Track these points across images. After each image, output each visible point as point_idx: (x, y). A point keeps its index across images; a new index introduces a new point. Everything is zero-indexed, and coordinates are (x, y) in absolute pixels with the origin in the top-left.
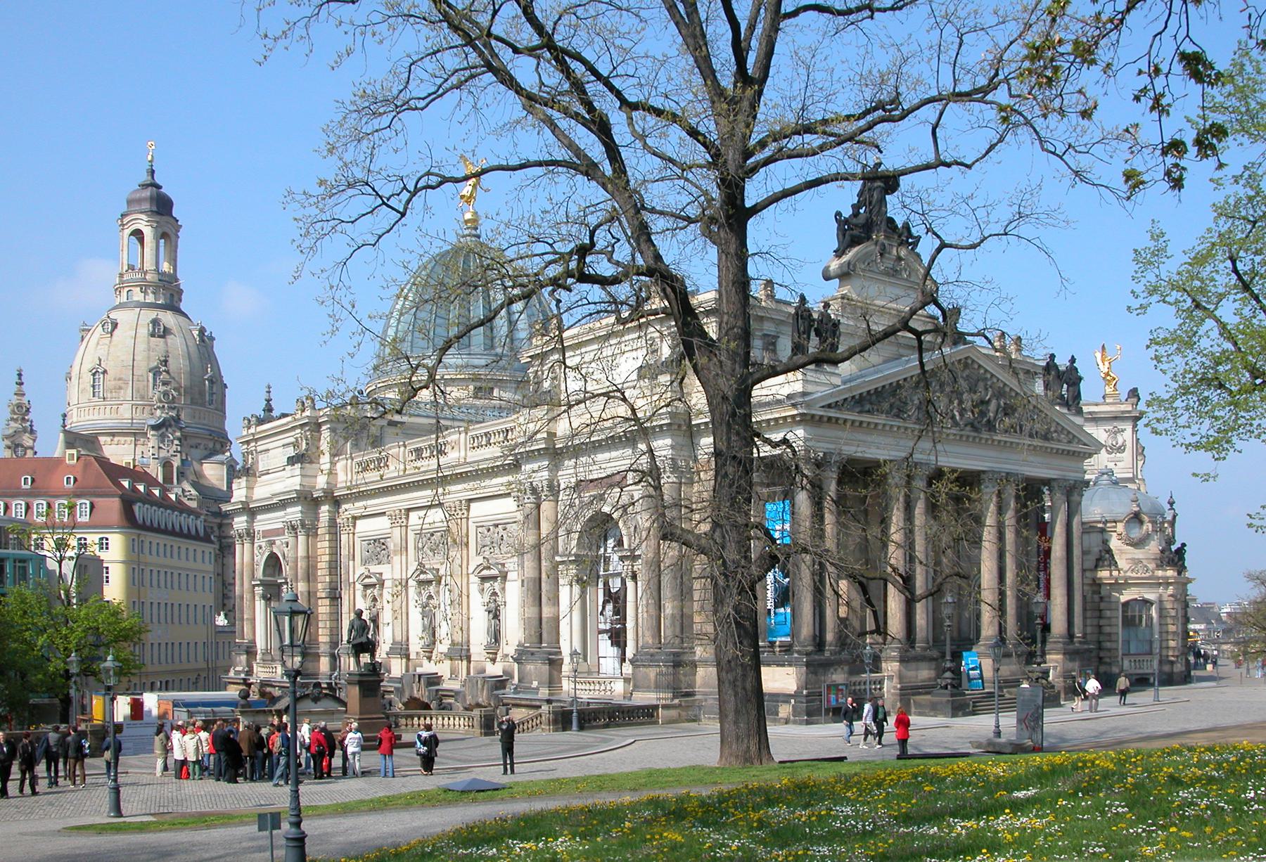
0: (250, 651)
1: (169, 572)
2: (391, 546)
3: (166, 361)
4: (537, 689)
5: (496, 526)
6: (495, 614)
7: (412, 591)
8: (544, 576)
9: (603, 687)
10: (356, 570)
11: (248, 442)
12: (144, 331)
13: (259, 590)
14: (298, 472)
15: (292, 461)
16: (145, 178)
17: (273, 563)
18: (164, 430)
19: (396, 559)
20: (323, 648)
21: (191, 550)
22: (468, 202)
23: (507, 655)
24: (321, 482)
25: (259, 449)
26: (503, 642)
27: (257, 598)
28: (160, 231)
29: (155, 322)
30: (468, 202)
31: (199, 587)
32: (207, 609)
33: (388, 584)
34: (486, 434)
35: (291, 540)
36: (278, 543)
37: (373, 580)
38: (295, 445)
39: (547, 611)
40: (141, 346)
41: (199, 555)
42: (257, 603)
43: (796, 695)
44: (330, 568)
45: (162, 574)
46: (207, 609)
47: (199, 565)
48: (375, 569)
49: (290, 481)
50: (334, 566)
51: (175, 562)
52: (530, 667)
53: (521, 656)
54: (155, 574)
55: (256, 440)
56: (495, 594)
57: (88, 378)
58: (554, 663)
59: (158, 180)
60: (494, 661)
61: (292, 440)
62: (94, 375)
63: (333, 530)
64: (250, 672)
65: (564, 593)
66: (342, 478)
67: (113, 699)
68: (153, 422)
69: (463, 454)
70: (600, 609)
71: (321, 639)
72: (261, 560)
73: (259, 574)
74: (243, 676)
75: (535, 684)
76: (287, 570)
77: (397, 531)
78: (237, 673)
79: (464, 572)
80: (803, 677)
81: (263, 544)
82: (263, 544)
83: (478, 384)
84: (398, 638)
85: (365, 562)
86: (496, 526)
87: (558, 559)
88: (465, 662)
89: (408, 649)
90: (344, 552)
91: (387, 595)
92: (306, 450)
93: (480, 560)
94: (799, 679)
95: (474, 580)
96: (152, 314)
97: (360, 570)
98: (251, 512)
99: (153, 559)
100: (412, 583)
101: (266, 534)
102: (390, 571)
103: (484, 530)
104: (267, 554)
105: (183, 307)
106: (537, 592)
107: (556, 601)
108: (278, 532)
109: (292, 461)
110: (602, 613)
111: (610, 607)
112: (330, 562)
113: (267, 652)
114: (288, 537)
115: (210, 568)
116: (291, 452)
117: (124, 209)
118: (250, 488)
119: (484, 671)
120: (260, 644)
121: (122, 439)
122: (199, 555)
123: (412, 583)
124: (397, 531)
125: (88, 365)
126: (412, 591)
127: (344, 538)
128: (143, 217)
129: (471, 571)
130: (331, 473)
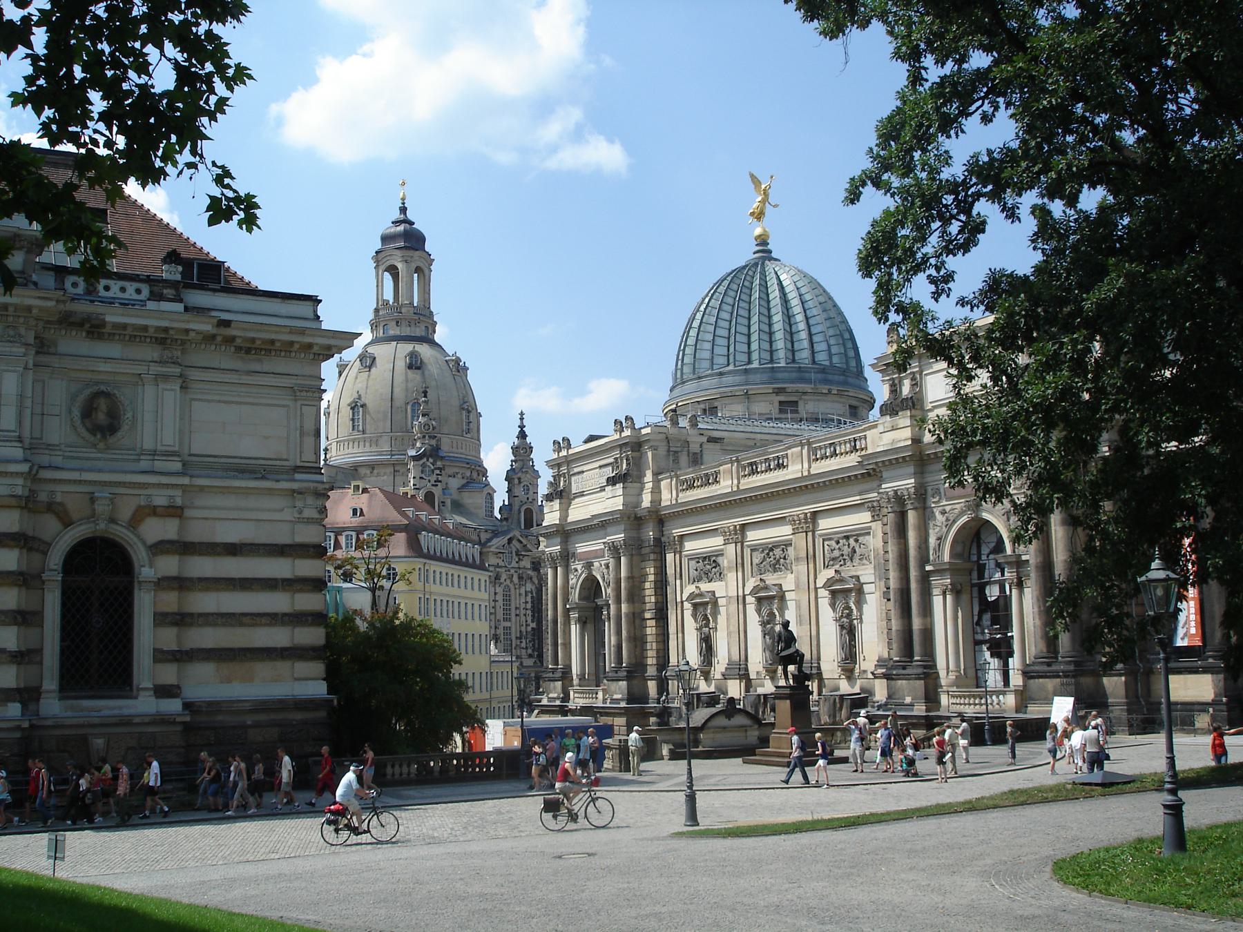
0: (566, 675)
3: (425, 394)
4: (912, 705)
5: (847, 538)
6: (849, 631)
9: (983, 701)
10: (683, 590)
11: (559, 465)
12: (401, 364)
13: (574, 615)
14: (620, 492)
15: (612, 481)
16: (397, 215)
17: (592, 588)
19: (731, 576)
20: (651, 671)
22: (759, 218)
23: (865, 671)
26: (860, 657)
27: (573, 622)
28: (414, 266)
29: (413, 355)
30: (759, 218)
32: (483, 638)
36: (596, 564)
40: (399, 378)
42: (573, 627)
43: (1214, 703)
46: (483, 638)
47: (476, 594)
48: (705, 587)
49: (613, 501)
50: (662, 585)
57: (346, 412)
58: (929, 674)
59: (410, 216)
61: (611, 460)
62: (353, 408)
63: (658, 550)
64: (566, 698)
65: (937, 601)
66: (667, 498)
67: (889, 697)
68: (412, 453)
70: (976, 618)
71: (650, 661)
73: (575, 596)
74: (558, 703)
75: (908, 700)
76: (608, 592)
77: (731, 549)
78: (550, 699)
79: (812, 586)
80: (1221, 684)
81: (579, 567)
82: (579, 567)
83: (782, 398)
84: (736, 657)
86: (847, 538)
87: (928, 568)
89: (747, 669)
93: (830, 573)
94: (1215, 686)
95: (823, 593)
96: (409, 347)
97: (690, 589)
98: (565, 533)
99: (435, 588)
100: (750, 600)
102: (724, 588)
103: (833, 543)
104: (584, 576)
105: (437, 338)
106: (907, 603)
107: (927, 610)
108: (598, 554)
109: (612, 481)
110: (978, 623)
111: (987, 618)
115: (486, 596)
116: (609, 472)
117: (379, 246)
119: (837, 689)
120: (575, 670)
121: (382, 471)
123: (750, 599)
125: (347, 399)
127: (670, 557)
128: (398, 252)
129: (820, 583)
130: (656, 490)
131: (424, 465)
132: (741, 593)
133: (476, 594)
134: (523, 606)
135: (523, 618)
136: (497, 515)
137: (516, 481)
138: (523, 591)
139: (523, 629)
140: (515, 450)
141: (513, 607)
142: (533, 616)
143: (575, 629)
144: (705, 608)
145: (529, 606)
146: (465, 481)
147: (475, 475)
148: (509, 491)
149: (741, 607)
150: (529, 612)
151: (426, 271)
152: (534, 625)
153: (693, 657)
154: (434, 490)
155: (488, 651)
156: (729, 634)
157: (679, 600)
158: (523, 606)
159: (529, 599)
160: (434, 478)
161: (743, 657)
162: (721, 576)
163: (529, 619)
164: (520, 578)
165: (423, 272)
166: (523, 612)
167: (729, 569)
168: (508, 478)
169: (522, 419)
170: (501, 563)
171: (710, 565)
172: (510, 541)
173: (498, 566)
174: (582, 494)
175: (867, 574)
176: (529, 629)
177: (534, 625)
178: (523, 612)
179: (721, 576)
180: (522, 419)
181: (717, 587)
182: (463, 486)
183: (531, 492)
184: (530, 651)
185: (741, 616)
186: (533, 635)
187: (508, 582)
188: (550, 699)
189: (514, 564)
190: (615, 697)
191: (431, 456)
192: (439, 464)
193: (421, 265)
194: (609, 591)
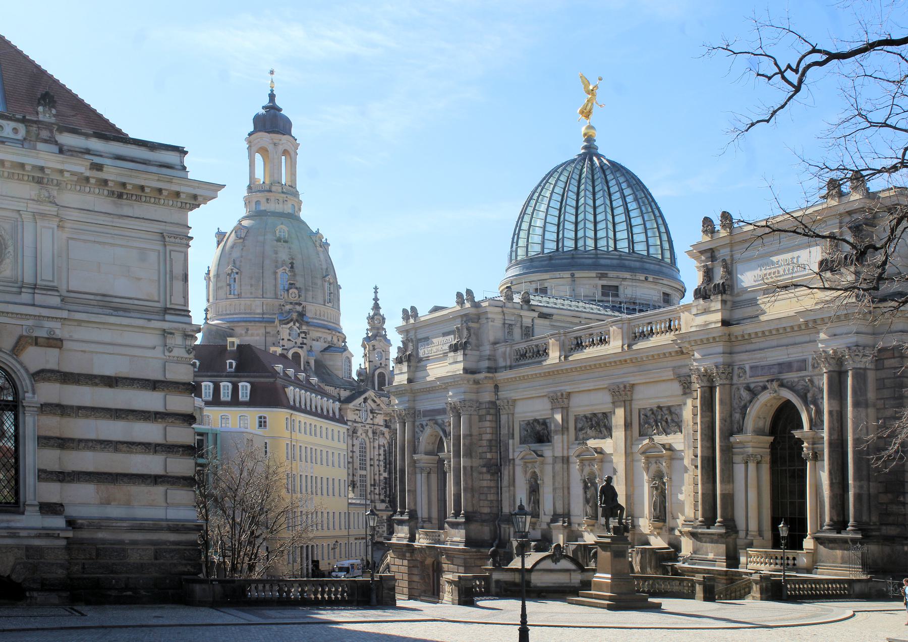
1: (309, 447)
18: (292, 324)
131: (290, 329)
133: (335, 444)
134: (376, 457)
135: (377, 468)
136: (355, 376)
138: (376, 445)
139: (377, 477)
140: (371, 319)
142: (385, 467)
145: (382, 458)
146: (326, 345)
150: (382, 463)
152: (386, 475)
155: (346, 496)
158: (376, 457)
159: (382, 452)
163: (382, 469)
164: (374, 433)
169: (376, 292)
170: (358, 420)
172: (365, 400)
173: (355, 422)
176: (382, 478)
177: (386, 475)
178: (376, 463)
180: (376, 292)
182: (326, 349)
183: (384, 359)
184: (382, 497)
186: (386, 483)
187: (364, 435)
189: (369, 421)
191: (297, 321)
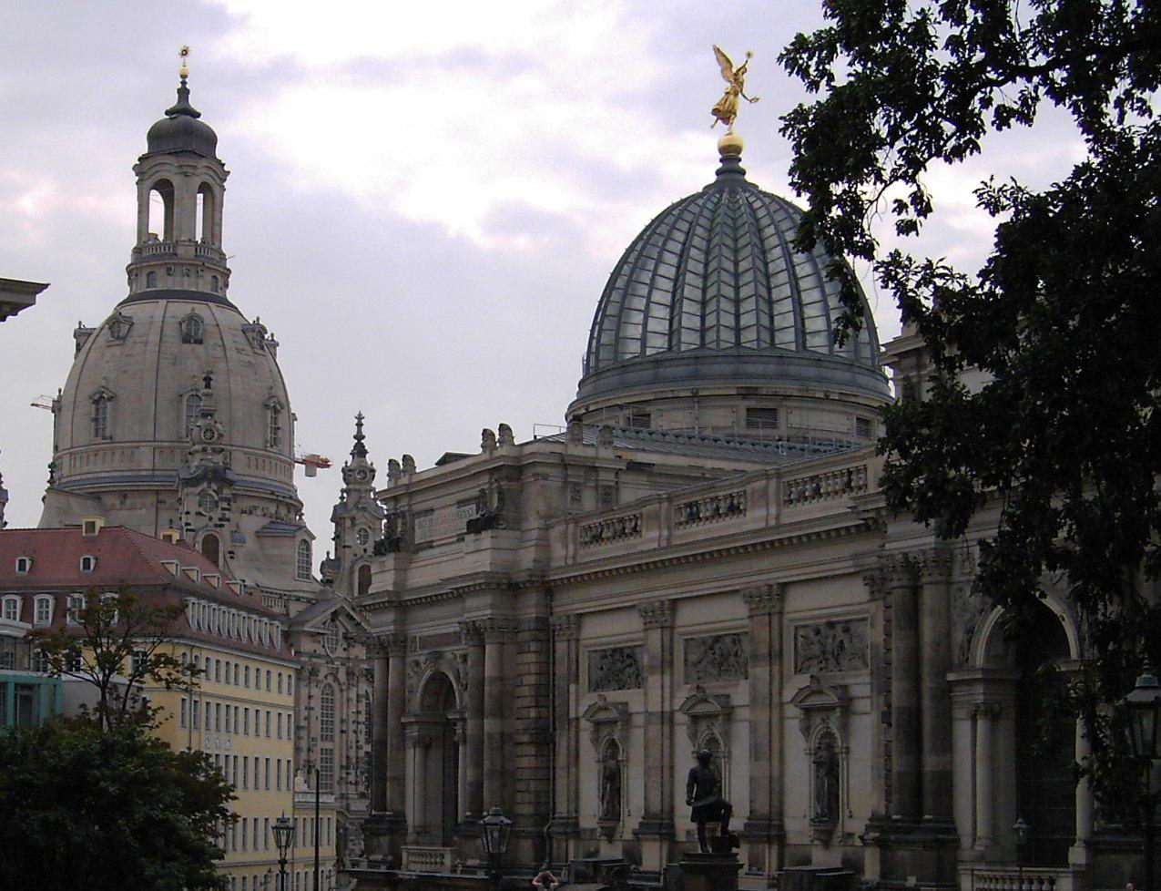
2: (646, 660)
3: (208, 380)
6: (828, 766)
7: (682, 734)
8: (926, 702)
10: (582, 701)
11: (396, 499)
15: (475, 527)
16: (173, 101)
19: (653, 681)
21: (264, 669)
23: (851, 835)
24: (527, 558)
25: (417, 508)
26: (843, 814)
27: (409, 743)
28: (197, 181)
31: (274, 731)
33: (639, 720)
34: (812, 479)
35: (472, 652)
37: (613, 714)
38: (481, 499)
39: (930, 762)
41: (274, 678)
44: (537, 696)
45: (223, 710)
47: (273, 697)
48: (614, 696)
51: (240, 692)
52: (903, 854)
53: (884, 832)
54: (213, 708)
55: (410, 495)
56: (829, 735)
59: (194, 102)
60: (827, 844)
61: (475, 492)
62: (96, 402)
63: (542, 636)
64: (396, 863)
65: (962, 730)
69: (773, 510)
72: (418, 683)
73: (415, 702)
74: (383, 869)
76: (462, 698)
79: (776, 700)
81: (422, 659)
83: (752, 403)
85: (596, 686)
87: (951, 677)
88: (775, 849)
89: (672, 826)
90: (561, 670)
91: (637, 736)
92: (500, 508)
95: (792, 711)
97: (589, 699)
100: (681, 718)
101: (425, 643)
104: (428, 673)
105: (231, 295)
106: (914, 731)
107: (945, 743)
109: (475, 527)
112: (538, 686)
113: (423, 830)
114: (462, 648)
115: (290, 701)
116: (471, 512)
118: (401, 570)
119: (808, 861)
120: (412, 817)
122: (274, 678)
123: (681, 718)
124: (655, 638)
126: (682, 734)
127: (561, 647)
129: (789, 694)
130: (544, 544)
131: (202, 494)
132: (667, 708)
134: (353, 717)
135: (352, 736)
137: (348, 523)
138: (353, 695)
139: (352, 753)
141: (337, 719)
143: (412, 757)
144: (611, 728)
145: (362, 718)
146: (266, 521)
147: (283, 511)
148: (337, 538)
149: (666, 728)
150: (362, 727)
151: (216, 189)
153: (590, 810)
154: (217, 532)
156: (647, 771)
157: (572, 715)
159: (362, 707)
160: (217, 514)
161: (667, 808)
162: (639, 681)
163: (362, 738)
164: (349, 674)
165: (212, 191)
166: (353, 727)
167: (652, 669)
168: (336, 518)
169: (359, 425)
170: (321, 651)
171: (620, 666)
173: (314, 655)
174: (429, 545)
175: (861, 685)
176: (361, 754)
178: (353, 727)
179: (639, 681)
180: (359, 425)
181: (634, 699)
184: (362, 788)
185: (667, 743)
186: (369, 763)
187: (330, 680)
188: (372, 864)
190: (470, 862)
192: (227, 492)
193: (211, 181)
194: (466, 696)
